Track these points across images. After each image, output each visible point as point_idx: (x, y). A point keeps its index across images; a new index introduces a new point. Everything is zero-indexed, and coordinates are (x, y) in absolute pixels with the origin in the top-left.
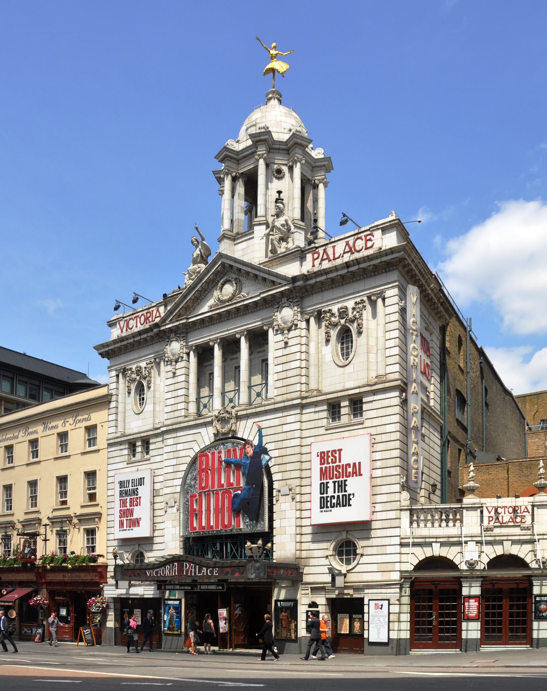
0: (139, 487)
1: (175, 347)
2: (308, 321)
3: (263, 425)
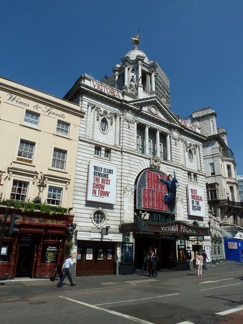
0: (109, 174)
1: (129, 116)
3: (175, 171)
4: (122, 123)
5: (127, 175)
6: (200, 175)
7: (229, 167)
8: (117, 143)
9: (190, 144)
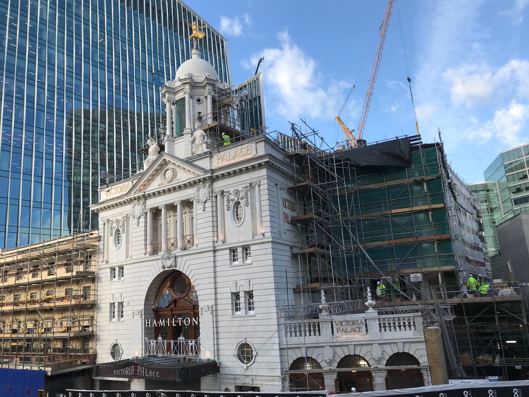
2: (216, 197)
9: (237, 192)
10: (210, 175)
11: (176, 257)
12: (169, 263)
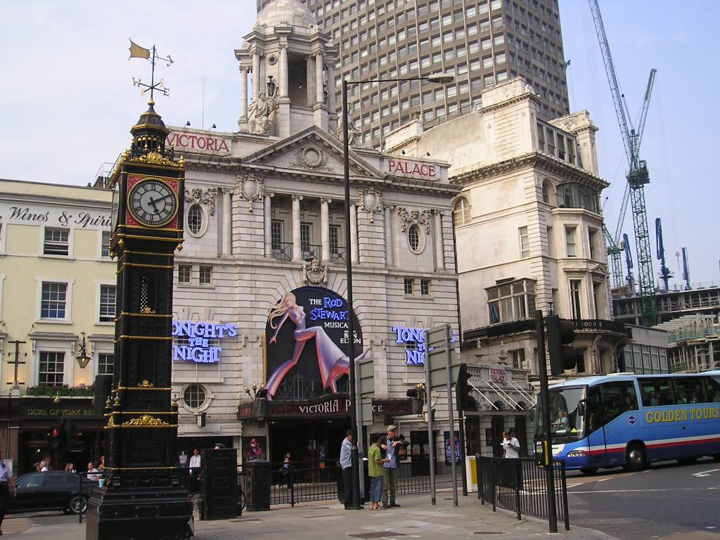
4: (235, 205)
5: (250, 311)
6: (440, 279)
7: (570, 230)
8: (225, 250)
10: (390, 182)
11: (329, 271)
12: (315, 278)
